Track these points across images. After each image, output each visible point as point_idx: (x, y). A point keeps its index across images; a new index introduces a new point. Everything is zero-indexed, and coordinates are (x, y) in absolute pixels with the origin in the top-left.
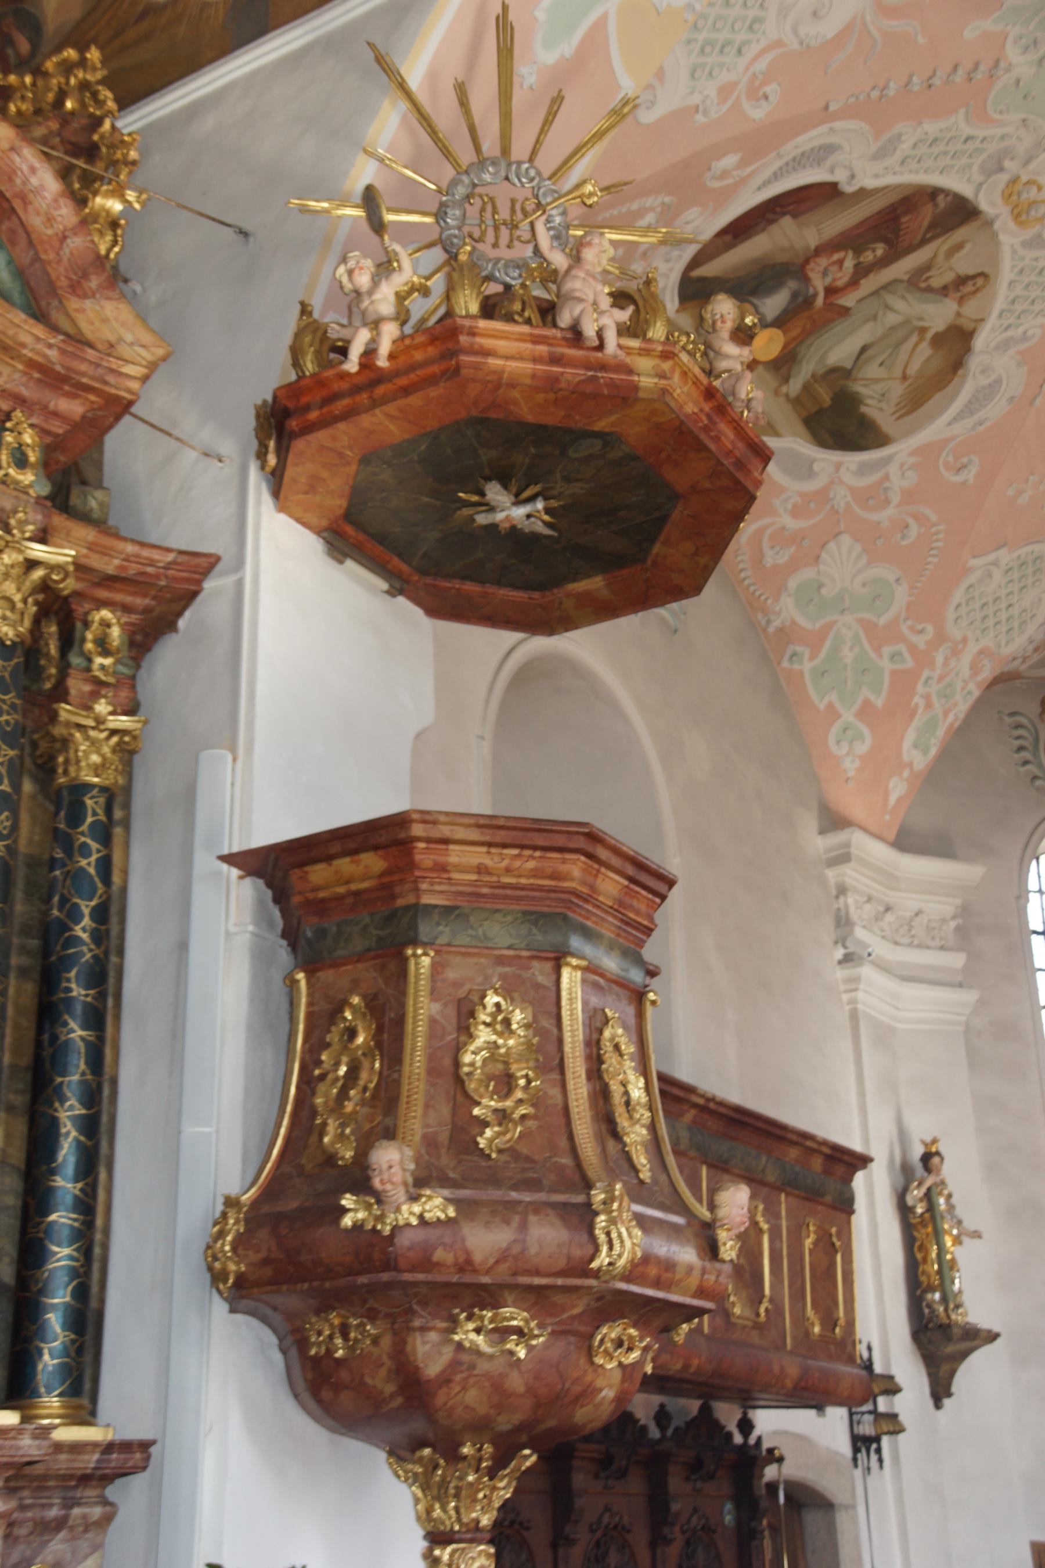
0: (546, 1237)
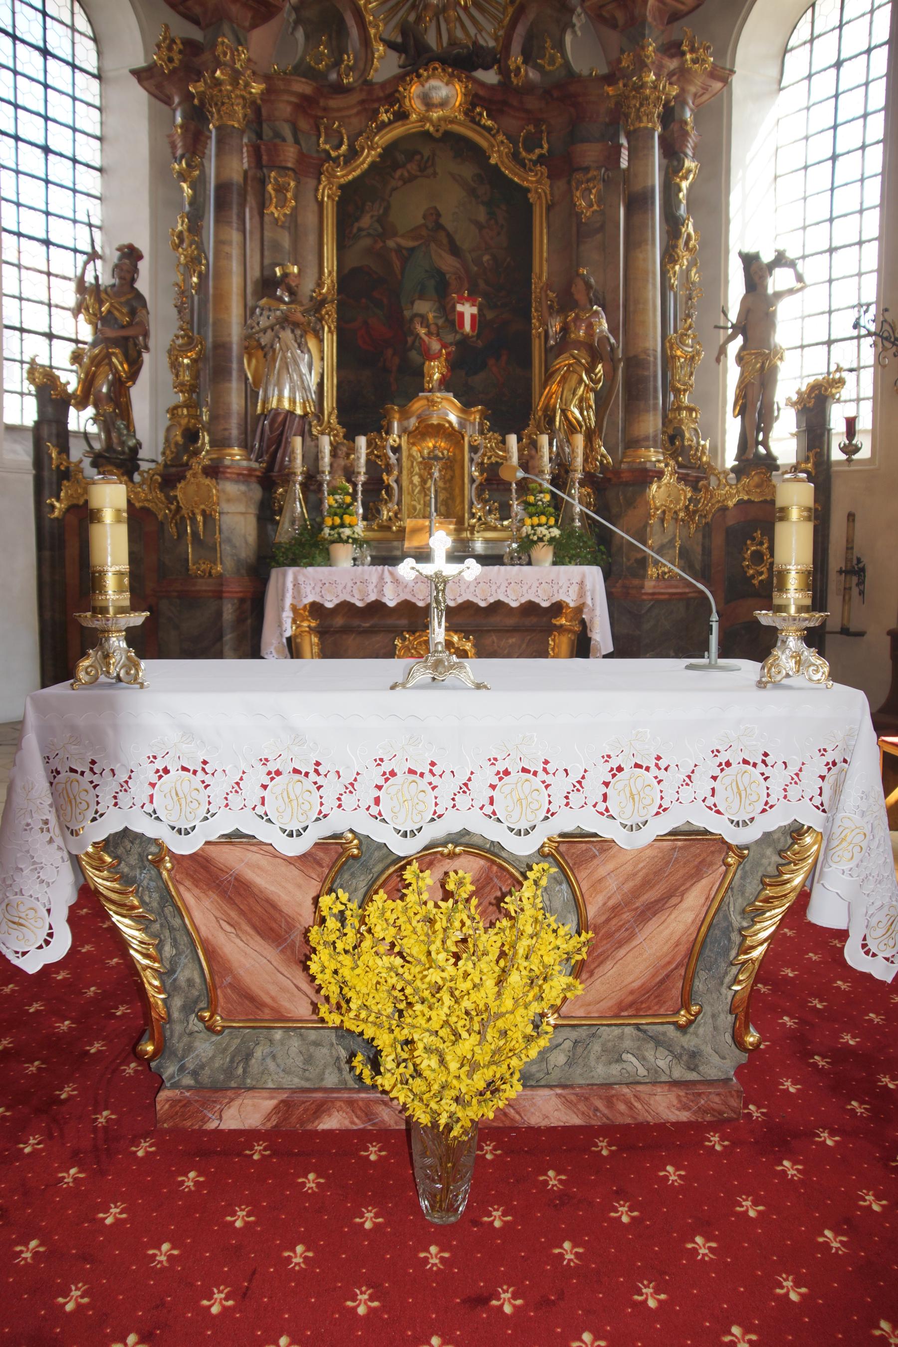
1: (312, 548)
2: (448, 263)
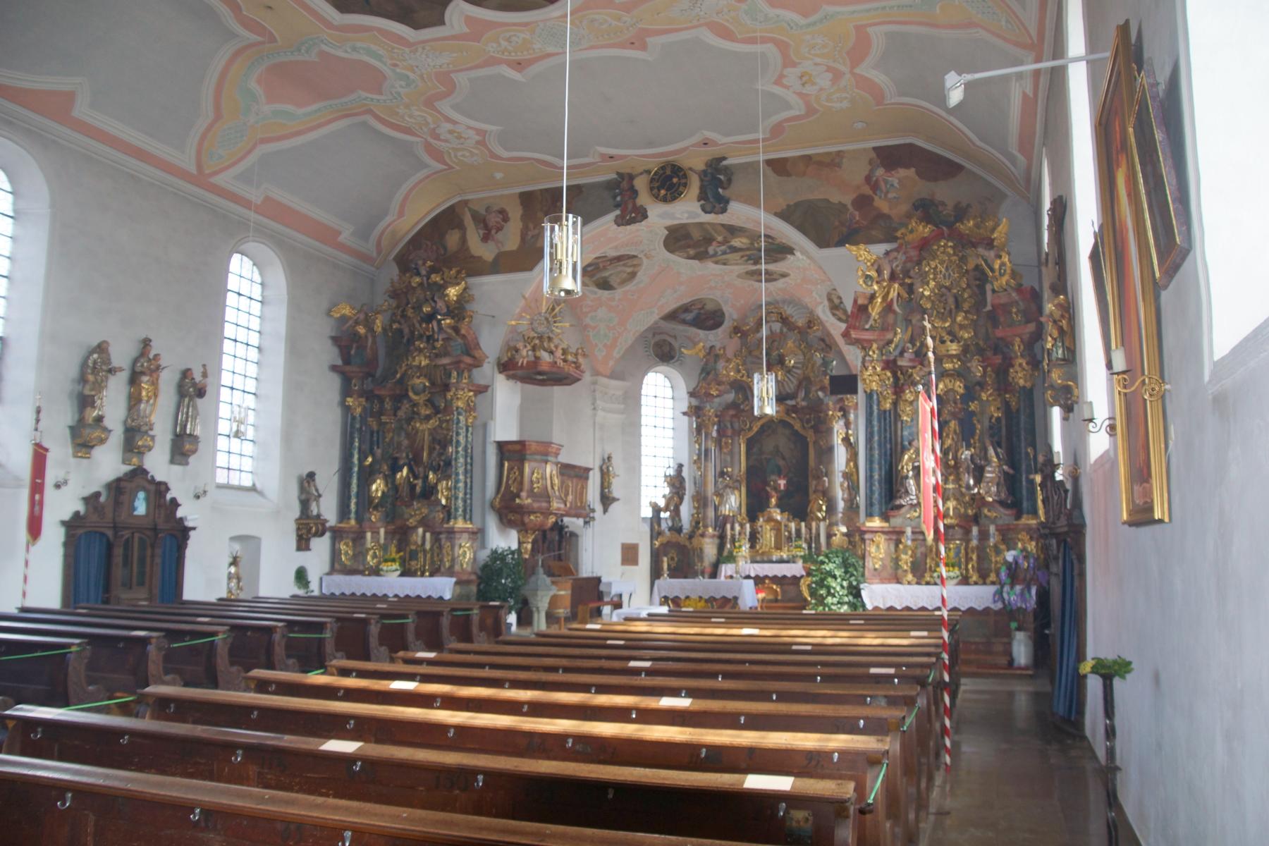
0: (544, 505)
1: (731, 558)
2: (781, 463)
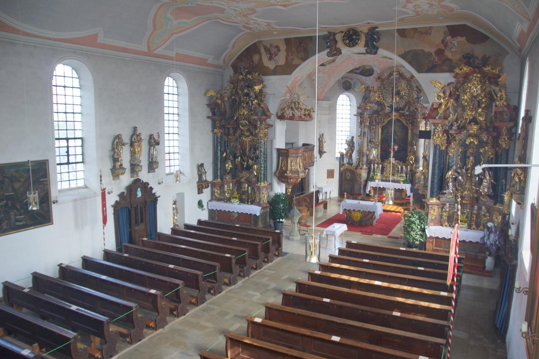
0: (296, 175)
1: (373, 179)
